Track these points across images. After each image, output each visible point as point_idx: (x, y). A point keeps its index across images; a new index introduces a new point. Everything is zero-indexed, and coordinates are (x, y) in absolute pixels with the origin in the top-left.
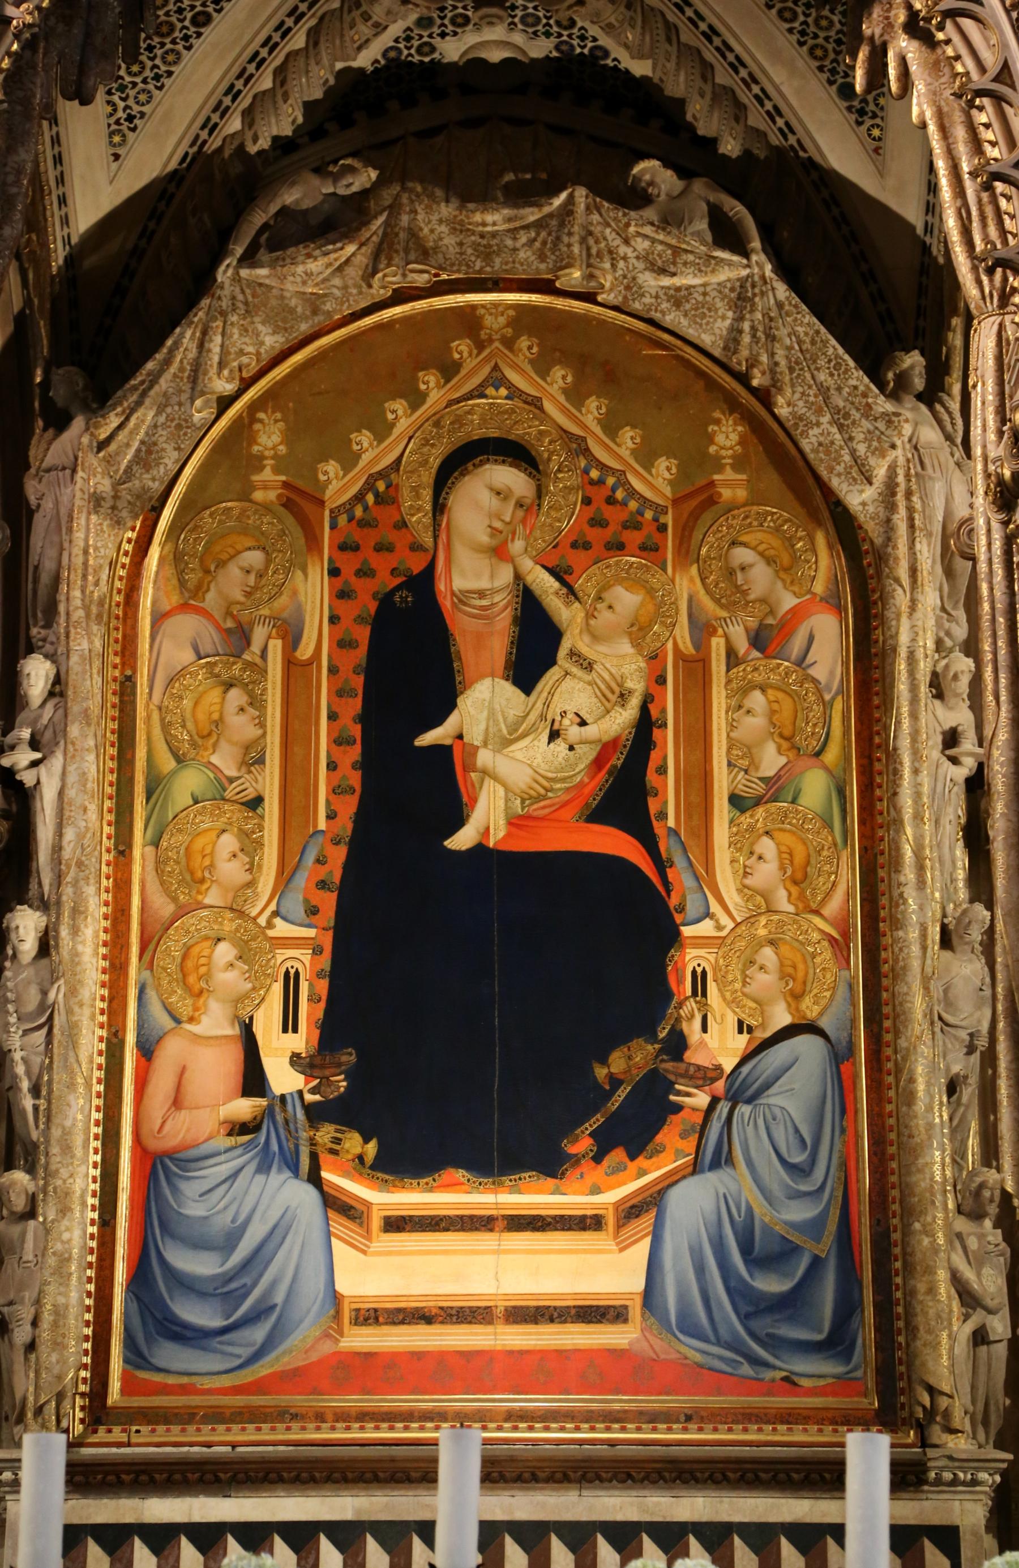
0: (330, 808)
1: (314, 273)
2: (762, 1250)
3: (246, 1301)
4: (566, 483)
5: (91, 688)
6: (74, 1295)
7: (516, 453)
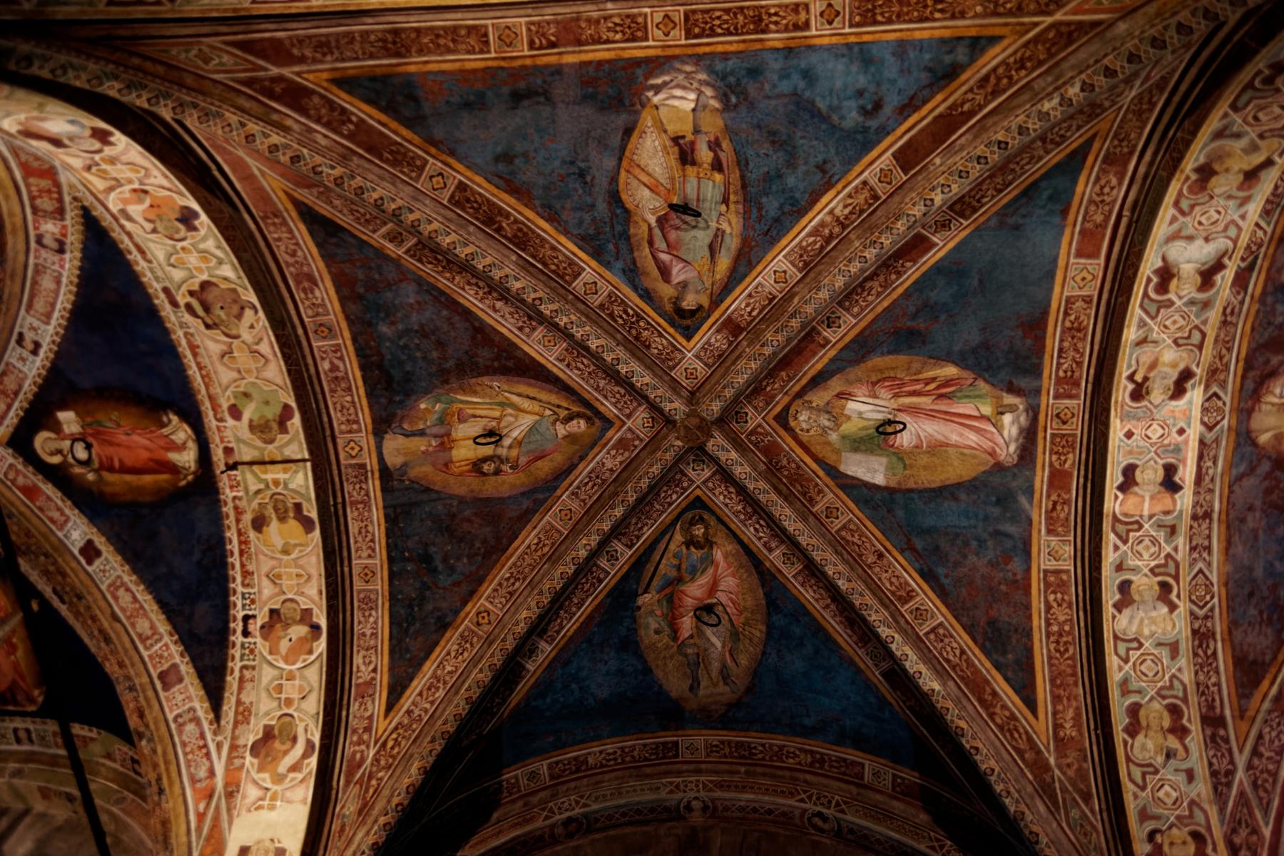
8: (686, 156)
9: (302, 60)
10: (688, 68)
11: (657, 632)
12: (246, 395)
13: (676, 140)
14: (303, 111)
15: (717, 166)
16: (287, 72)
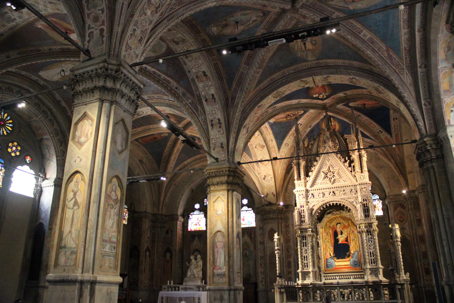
0: (333, 242)
1: (329, 215)
2: (355, 262)
3: (331, 265)
4: (342, 225)
5: (321, 237)
6: (323, 266)
7: (340, 223)
8: (226, 25)
9: (227, 96)
10: (207, 31)
11: (362, 4)
12: (299, 86)
13: (223, 28)
14: (235, 97)
15: (226, 20)
16: (230, 99)
